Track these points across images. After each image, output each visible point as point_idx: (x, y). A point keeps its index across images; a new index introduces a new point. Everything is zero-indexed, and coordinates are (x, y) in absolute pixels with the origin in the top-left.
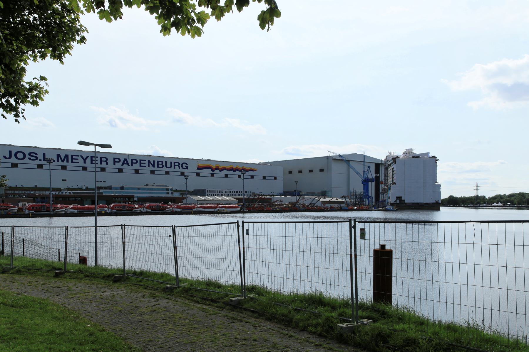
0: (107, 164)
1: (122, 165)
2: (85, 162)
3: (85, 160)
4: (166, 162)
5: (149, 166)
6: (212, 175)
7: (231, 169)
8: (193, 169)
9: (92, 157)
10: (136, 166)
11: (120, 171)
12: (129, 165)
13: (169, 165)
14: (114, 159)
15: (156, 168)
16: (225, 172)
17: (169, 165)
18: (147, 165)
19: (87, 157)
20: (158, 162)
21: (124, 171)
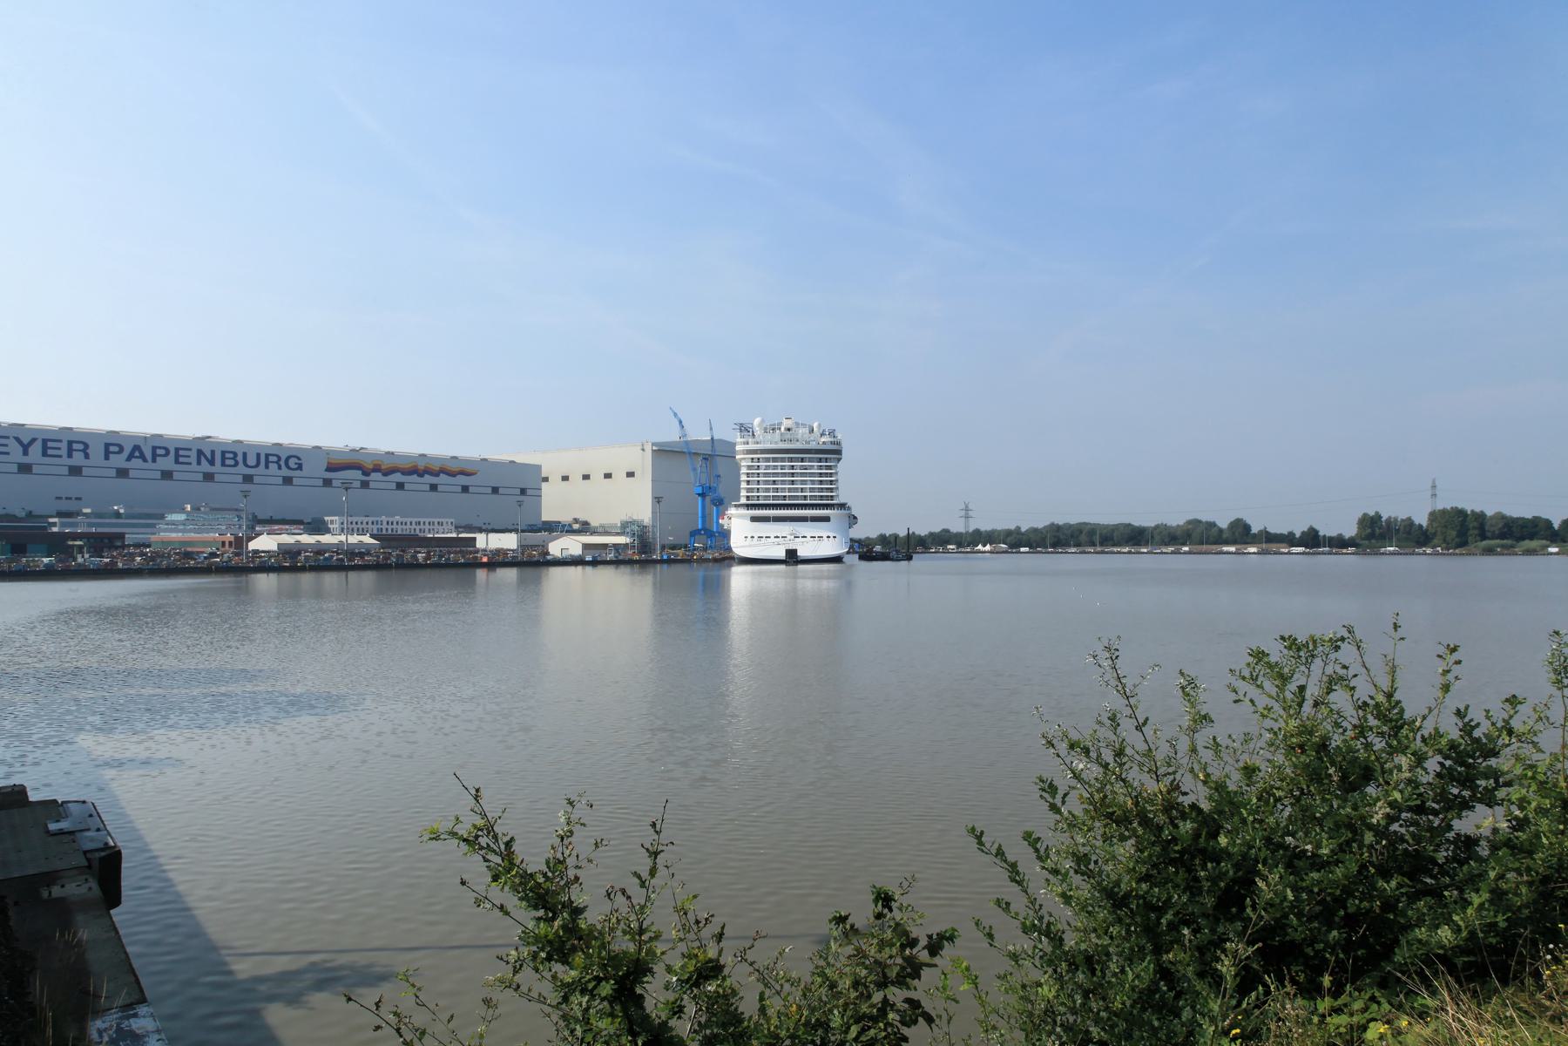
0: (87, 456)
1: (129, 459)
2: (25, 453)
3: (26, 450)
4: (245, 455)
5: (199, 463)
6: (365, 485)
7: (414, 471)
8: (316, 470)
9: (45, 441)
10: (166, 463)
11: (122, 473)
12: (145, 460)
13: (252, 461)
14: (107, 446)
15: (218, 467)
16: (398, 477)
17: (252, 461)
18: (193, 459)
19: (34, 440)
20: (223, 453)
21: (132, 474)
